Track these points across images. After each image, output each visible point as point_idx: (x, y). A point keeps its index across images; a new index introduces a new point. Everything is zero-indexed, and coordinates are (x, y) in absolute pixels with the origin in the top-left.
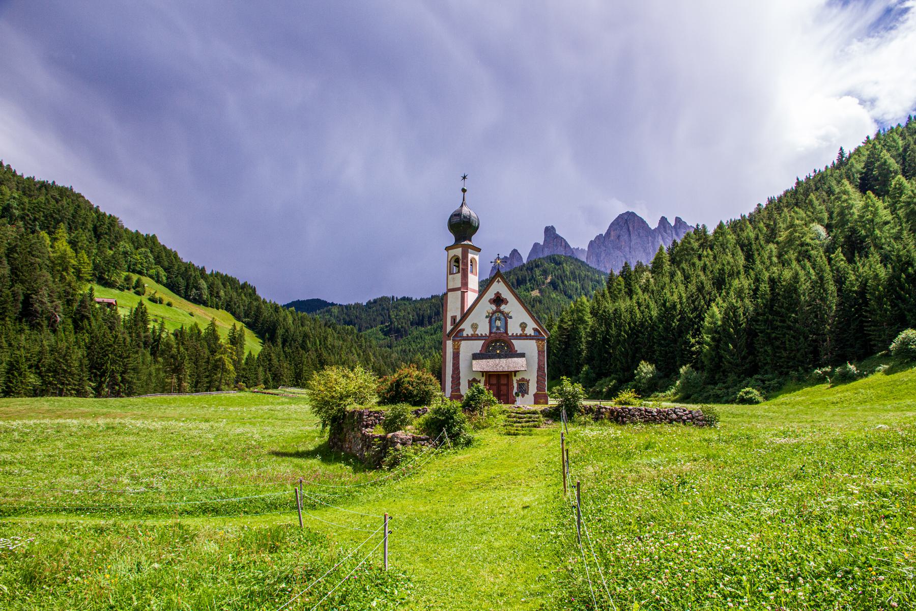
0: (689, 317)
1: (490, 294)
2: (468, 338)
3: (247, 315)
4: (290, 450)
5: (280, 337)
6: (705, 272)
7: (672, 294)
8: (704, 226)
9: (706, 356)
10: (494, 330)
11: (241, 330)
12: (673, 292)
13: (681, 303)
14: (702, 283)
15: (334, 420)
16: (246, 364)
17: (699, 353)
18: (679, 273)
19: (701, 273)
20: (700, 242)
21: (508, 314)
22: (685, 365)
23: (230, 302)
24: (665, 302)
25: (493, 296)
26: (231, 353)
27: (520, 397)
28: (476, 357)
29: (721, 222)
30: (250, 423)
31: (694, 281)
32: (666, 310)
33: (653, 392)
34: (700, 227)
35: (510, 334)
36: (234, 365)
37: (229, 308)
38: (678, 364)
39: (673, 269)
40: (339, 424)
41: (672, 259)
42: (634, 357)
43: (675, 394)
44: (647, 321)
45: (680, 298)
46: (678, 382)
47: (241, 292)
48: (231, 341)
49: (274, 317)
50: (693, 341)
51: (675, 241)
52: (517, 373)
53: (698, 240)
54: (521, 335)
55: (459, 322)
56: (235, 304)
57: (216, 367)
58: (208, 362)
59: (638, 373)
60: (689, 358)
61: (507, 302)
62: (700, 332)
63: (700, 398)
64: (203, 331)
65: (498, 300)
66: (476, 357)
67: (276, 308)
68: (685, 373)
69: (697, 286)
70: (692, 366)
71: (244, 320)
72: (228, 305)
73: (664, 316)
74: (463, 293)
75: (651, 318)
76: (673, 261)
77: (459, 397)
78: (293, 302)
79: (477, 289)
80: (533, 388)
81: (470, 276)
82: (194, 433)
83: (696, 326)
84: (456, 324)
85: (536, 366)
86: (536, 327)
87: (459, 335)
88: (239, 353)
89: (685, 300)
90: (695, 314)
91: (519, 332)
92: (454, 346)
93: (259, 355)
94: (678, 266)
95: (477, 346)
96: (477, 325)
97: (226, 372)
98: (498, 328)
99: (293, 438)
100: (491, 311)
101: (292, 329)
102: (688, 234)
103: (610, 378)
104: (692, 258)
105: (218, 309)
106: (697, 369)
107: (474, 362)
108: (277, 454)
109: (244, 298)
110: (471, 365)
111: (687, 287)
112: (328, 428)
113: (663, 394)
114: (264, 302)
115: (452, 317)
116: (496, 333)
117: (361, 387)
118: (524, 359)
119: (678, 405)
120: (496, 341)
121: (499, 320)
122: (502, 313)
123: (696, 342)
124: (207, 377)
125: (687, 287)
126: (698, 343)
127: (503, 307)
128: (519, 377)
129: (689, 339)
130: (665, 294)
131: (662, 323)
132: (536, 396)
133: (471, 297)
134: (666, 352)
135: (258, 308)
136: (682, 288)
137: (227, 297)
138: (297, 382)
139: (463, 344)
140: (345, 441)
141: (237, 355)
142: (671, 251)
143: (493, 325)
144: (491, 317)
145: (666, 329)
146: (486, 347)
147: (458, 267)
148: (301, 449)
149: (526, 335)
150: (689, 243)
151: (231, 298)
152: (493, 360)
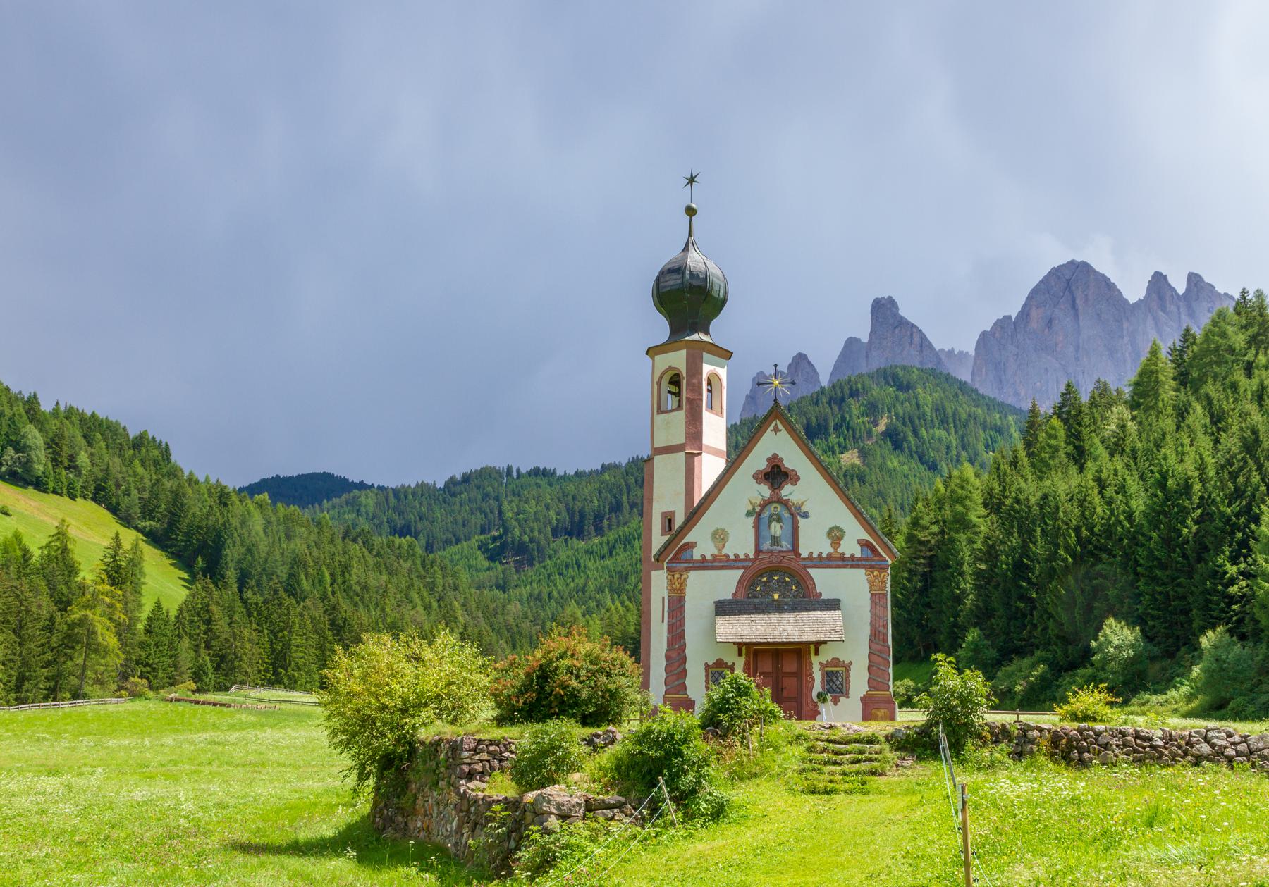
0: (1222, 514)
1: (757, 460)
2: (704, 565)
3: (148, 513)
4: (277, 838)
5: (232, 565)
6: (1261, 406)
7: (1181, 458)
8: (1259, 294)
9: (1263, 607)
10: (766, 545)
11: (135, 548)
12: (1183, 454)
13: (1203, 481)
14: (1255, 432)
15: (387, 762)
16: (148, 631)
17: (1244, 599)
18: (1198, 407)
19: (1253, 408)
20: (1251, 332)
21: (800, 508)
22: (1214, 628)
23: (105, 480)
24: (1164, 477)
25: (763, 465)
26: (111, 606)
27: (830, 703)
28: (723, 608)
30: (167, 776)
31: (1235, 428)
32: (1167, 498)
33: (1135, 691)
34: (1250, 296)
36: (119, 635)
37: (100, 494)
38: (1195, 625)
39: (1183, 398)
40: (400, 771)
41: (1181, 374)
42: (1089, 609)
43: (1190, 698)
44: (1120, 522)
45: (1202, 467)
46: (1196, 670)
47: (134, 456)
48: (109, 577)
49: (217, 518)
50: (1232, 570)
51: (1187, 330)
52: (821, 648)
53: (1245, 327)
54: (830, 557)
55: (681, 528)
56: (118, 486)
57: (70, 640)
58: (50, 629)
59: (1100, 649)
60: (1222, 610)
61: (798, 479)
62: (1250, 550)
63: (1251, 708)
64: (36, 553)
65: (776, 474)
66: (723, 608)
67: (223, 497)
68: (1215, 647)
69: (1243, 439)
70: (1229, 631)
71: (141, 524)
72: (99, 488)
73: (1163, 512)
74: (691, 457)
75: (1130, 517)
76: (1183, 379)
77: (689, 705)
78: (263, 480)
79: (723, 447)
80: (859, 684)
81: (707, 417)
82: (24, 802)
83: (1239, 535)
84: (676, 532)
85: (866, 631)
86: (865, 536)
87: (684, 556)
88: (131, 606)
89: (1212, 473)
90: (1236, 507)
91: (826, 549)
92: (671, 582)
93: (181, 610)
94: (1196, 391)
95: (726, 583)
96: (724, 532)
97: (96, 651)
98: (776, 541)
99: (279, 810)
100: (759, 500)
101: (263, 547)
102: (1221, 315)
103: (1034, 659)
104: (1230, 371)
105: (73, 497)
106: (1243, 637)
107: (720, 621)
108: (245, 848)
109: (140, 470)
110: (713, 629)
111: (1217, 441)
112: (371, 782)
113: (1161, 698)
114: (192, 481)
115: (664, 515)
116: (771, 552)
117: (450, 683)
118: (838, 613)
119: (1200, 724)
120: (772, 571)
121: (779, 520)
122: (785, 503)
123: (1242, 573)
124: (48, 664)
125: (1217, 441)
126: (1246, 575)
127: (787, 491)
128: (826, 655)
129: (1221, 566)
130: (1165, 458)
131: (1156, 528)
132: (867, 701)
133: (710, 468)
134: (1167, 595)
135: (177, 496)
136: (1205, 442)
137: (96, 470)
138: (276, 673)
139: (695, 579)
140: (414, 813)
141: (126, 611)
142: (1178, 357)
143: (764, 533)
144: (759, 515)
145: (1168, 542)
146: (747, 584)
147: (678, 394)
148: (303, 836)
149: (842, 557)
150: (1223, 335)
151: (107, 470)
152: (765, 616)
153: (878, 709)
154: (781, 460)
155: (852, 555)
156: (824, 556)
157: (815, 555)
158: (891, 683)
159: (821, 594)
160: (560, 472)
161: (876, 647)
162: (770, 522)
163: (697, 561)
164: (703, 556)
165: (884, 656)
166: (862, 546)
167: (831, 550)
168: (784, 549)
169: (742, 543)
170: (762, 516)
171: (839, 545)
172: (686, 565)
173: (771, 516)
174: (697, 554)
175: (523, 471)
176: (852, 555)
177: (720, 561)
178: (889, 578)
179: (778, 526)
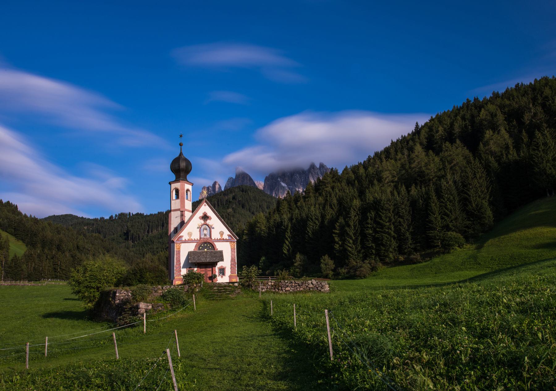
2: (185, 242)
25: (202, 215)
29: (346, 167)
54: (220, 239)
65: (205, 217)
80: (228, 272)
86: (230, 234)
87: (180, 240)
91: (219, 237)
98: (205, 235)
100: (201, 224)
120: (205, 243)
121: (206, 229)
122: (208, 225)
127: (208, 222)
149: (223, 239)
153: (233, 279)
154: (207, 213)
156: (219, 239)
157: (216, 239)
158: (236, 272)
160: (145, 214)
161: (232, 263)
162: (204, 230)
164: (185, 239)
169: (196, 236)
174: (183, 239)
175: (134, 214)
177: (190, 240)
179: (206, 231)
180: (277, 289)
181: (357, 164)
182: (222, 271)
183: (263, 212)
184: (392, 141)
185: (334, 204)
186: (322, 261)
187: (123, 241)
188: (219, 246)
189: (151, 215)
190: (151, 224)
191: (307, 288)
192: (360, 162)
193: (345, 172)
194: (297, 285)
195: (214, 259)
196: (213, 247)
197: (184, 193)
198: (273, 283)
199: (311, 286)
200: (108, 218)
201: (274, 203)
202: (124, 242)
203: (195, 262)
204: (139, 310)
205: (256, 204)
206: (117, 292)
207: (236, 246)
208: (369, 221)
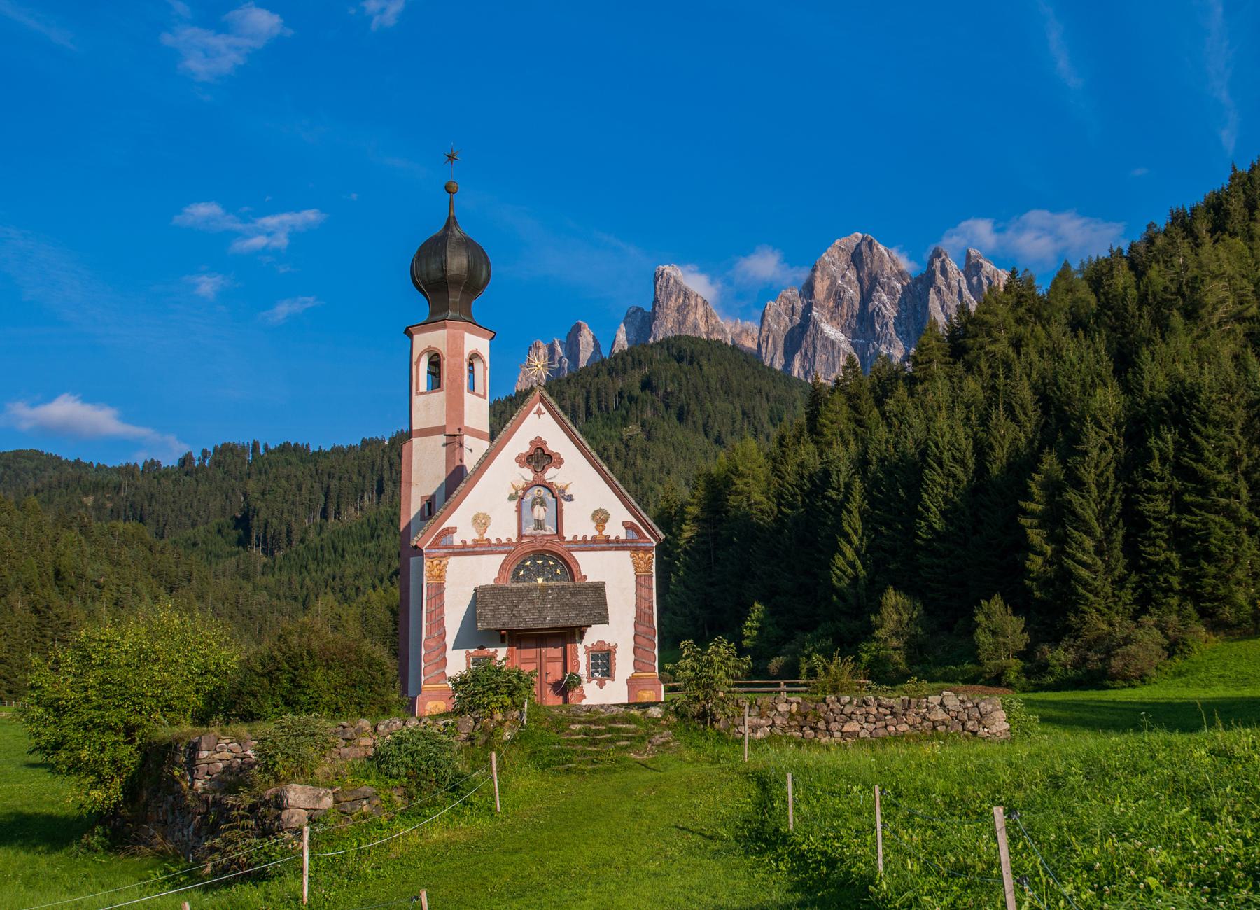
2: (465, 550)
10: (529, 530)
21: (563, 492)
25: (525, 448)
35: (569, 538)
54: (594, 540)
65: (539, 457)
80: (624, 665)
87: (443, 543)
91: (591, 531)
98: (539, 524)
100: (522, 484)
116: (535, 537)
120: (539, 554)
121: (543, 503)
122: (549, 487)
127: (551, 474)
149: (607, 540)
154: (545, 443)
155: (617, 538)
156: (589, 539)
157: (580, 539)
158: (656, 664)
159: (585, 577)
160: (314, 448)
161: (641, 629)
162: (533, 506)
163: (458, 547)
164: (464, 542)
165: (650, 637)
166: (627, 528)
167: (596, 533)
168: (548, 533)
169: (504, 527)
170: (525, 500)
171: (604, 528)
172: (446, 551)
173: (535, 499)
174: (457, 540)
175: (272, 447)
176: (617, 538)
177: (482, 546)
178: (654, 559)
179: (542, 509)
180: (812, 728)
181: (1106, 254)
182: (603, 662)
183: (755, 436)
184: (1234, 169)
185: (1022, 406)
186: (980, 618)
187: (228, 549)
188: (592, 566)
189: (337, 451)
190: (334, 484)
191: (926, 724)
192: (1115, 249)
193: (1062, 284)
194: (888, 712)
195: (572, 614)
196: (569, 569)
197: (462, 368)
198: (794, 708)
199: (940, 715)
200: (176, 465)
201: (798, 404)
202: (232, 554)
203: (499, 627)
204: (285, 814)
205: (731, 406)
206: (204, 745)
207: (654, 567)
208: (1155, 466)
